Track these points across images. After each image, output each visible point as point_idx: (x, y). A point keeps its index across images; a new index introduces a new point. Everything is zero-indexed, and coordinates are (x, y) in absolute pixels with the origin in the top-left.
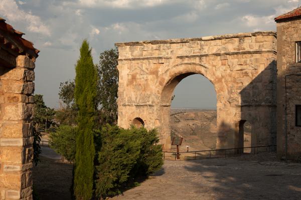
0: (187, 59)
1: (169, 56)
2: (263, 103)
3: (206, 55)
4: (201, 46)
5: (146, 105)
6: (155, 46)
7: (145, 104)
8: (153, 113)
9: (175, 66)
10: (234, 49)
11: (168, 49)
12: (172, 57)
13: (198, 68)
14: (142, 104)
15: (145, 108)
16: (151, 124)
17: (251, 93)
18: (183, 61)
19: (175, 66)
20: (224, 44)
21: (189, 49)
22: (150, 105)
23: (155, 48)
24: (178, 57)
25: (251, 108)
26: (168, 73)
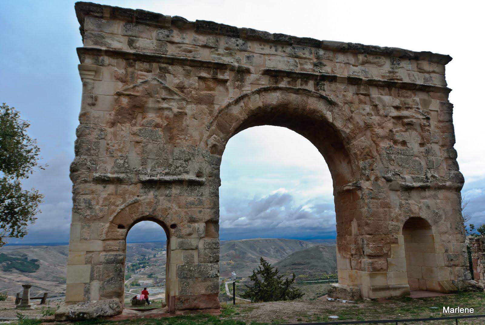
0: (286, 80)
1: (245, 64)
2: (448, 184)
3: (333, 79)
4: (318, 58)
5: (180, 182)
6: (203, 39)
7: (176, 177)
8: (201, 202)
9: (259, 92)
10: (383, 77)
11: (241, 50)
12: (252, 69)
13: (314, 104)
14: (168, 178)
15: (175, 191)
16: (195, 235)
17: (423, 163)
18: (276, 82)
19: (259, 92)
20: (363, 63)
21: (291, 60)
22: (191, 183)
23: (201, 43)
24: (267, 72)
25: (427, 193)
26: (242, 104)
